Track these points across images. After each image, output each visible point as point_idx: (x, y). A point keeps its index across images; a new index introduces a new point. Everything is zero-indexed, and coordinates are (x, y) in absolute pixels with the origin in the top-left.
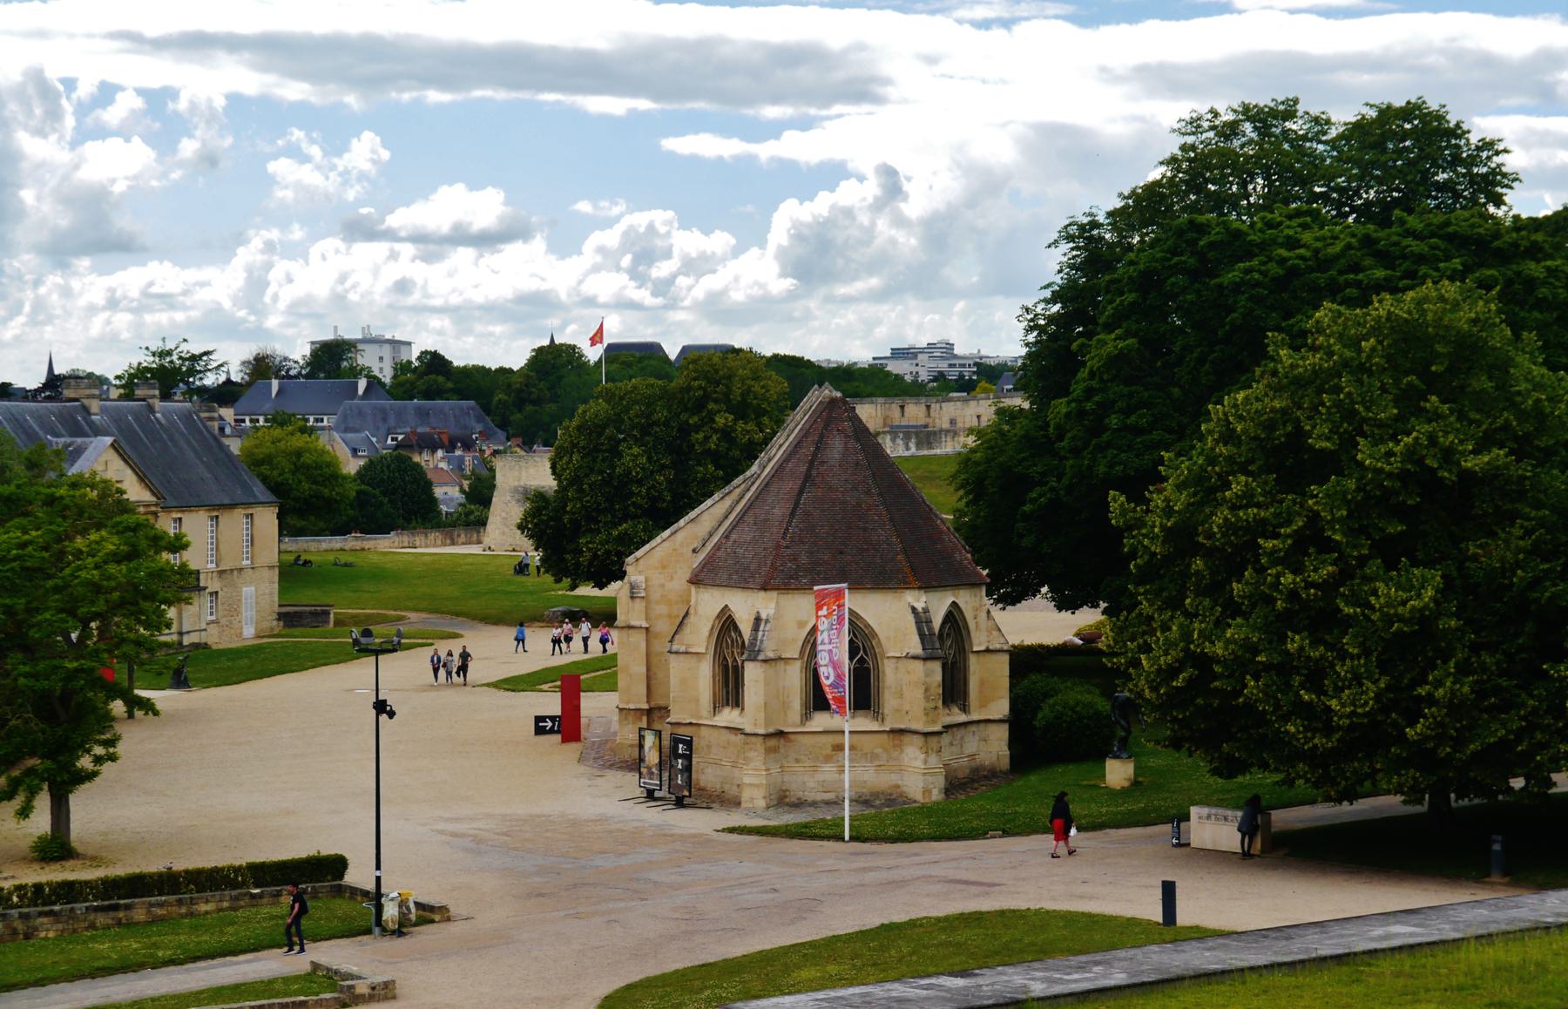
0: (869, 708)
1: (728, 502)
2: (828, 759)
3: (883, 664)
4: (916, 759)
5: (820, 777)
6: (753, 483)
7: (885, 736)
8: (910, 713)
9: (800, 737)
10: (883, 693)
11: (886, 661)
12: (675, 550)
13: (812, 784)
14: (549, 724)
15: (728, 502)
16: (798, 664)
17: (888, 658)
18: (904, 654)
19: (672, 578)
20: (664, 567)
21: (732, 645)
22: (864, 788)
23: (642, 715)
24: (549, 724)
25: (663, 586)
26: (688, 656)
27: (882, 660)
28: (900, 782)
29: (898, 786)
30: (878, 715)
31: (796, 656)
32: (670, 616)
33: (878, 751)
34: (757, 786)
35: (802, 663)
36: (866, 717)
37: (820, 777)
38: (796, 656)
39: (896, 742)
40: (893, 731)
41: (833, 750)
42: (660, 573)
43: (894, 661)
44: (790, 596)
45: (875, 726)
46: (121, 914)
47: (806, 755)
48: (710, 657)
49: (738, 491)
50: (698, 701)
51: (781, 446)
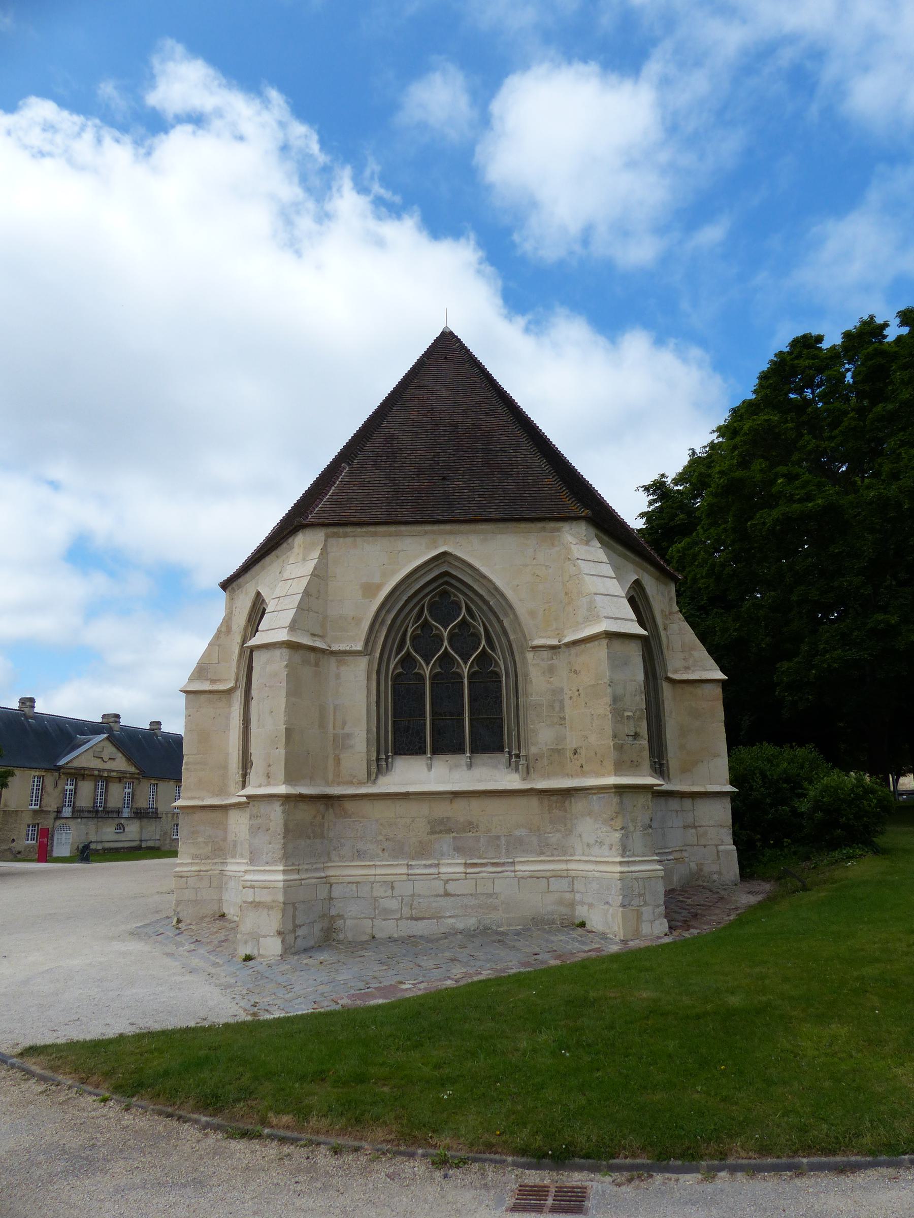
0: (500, 749)
3: (524, 659)
7: (534, 801)
8: (583, 752)
11: (530, 655)
17: (535, 648)
27: (522, 653)
31: (359, 647)
34: (268, 907)
35: (370, 663)
38: (359, 647)
43: (545, 654)
44: (349, 540)
45: (512, 781)
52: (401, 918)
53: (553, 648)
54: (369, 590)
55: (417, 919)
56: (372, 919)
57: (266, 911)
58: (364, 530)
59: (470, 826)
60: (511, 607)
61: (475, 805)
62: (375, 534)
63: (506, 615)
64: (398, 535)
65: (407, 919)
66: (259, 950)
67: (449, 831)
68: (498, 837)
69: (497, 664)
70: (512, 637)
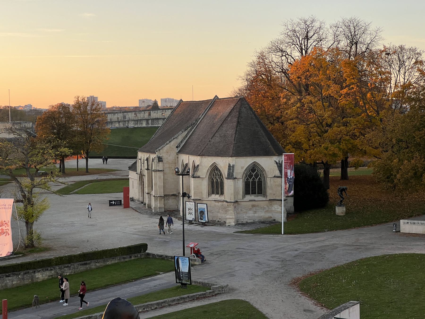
0: (262, 193)
1: (186, 132)
2: (250, 209)
4: (278, 209)
5: (248, 215)
6: (195, 126)
7: (267, 202)
9: (242, 203)
10: (267, 188)
11: (267, 179)
13: (246, 218)
14: (114, 203)
15: (186, 132)
16: (241, 180)
18: (273, 176)
19: (170, 156)
20: (167, 152)
23: (162, 198)
24: (114, 203)
25: (167, 158)
26: (199, 178)
28: (272, 216)
29: (271, 217)
30: (265, 195)
31: (241, 178)
32: (169, 168)
37: (248, 215)
40: (270, 200)
41: (252, 207)
42: (166, 154)
46: (88, 266)
48: (207, 179)
49: (189, 128)
50: (202, 193)
51: (203, 114)
54: (242, 168)
59: (258, 206)
63: (264, 172)
67: (254, 207)
68: (262, 208)
70: (265, 175)
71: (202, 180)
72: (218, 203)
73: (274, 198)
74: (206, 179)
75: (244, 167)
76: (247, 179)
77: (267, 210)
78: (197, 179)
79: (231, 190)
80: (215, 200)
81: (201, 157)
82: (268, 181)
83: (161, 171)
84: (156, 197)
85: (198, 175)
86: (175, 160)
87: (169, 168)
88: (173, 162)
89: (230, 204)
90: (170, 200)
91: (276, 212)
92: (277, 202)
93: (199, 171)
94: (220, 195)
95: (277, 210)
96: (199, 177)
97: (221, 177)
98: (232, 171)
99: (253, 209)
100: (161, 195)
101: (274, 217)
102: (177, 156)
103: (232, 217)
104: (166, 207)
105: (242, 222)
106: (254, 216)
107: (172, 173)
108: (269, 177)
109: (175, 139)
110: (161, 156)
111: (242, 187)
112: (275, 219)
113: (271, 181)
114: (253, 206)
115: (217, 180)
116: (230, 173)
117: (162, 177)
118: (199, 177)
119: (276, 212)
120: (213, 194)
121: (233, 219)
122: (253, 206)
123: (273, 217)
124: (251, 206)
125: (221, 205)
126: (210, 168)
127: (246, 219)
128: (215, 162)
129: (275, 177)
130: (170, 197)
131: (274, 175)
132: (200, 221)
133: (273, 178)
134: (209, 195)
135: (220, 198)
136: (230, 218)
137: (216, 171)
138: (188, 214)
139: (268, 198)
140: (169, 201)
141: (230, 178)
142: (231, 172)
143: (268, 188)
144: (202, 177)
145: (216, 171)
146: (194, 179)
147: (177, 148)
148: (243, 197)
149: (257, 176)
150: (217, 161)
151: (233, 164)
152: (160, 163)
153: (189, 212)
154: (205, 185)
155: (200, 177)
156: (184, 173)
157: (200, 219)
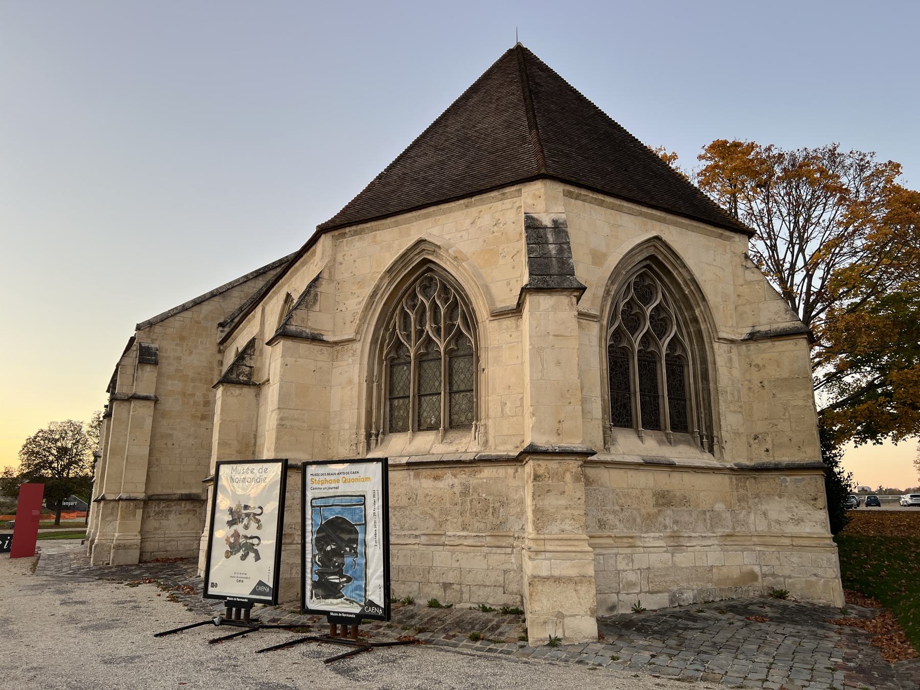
2: (649, 522)
4: (799, 521)
7: (723, 481)
11: (716, 345)
12: (197, 322)
13: (631, 577)
17: (719, 339)
20: (182, 339)
21: (421, 321)
22: (710, 581)
23: (136, 507)
25: (179, 358)
26: (315, 348)
28: (756, 569)
29: (753, 576)
30: (709, 442)
32: (183, 394)
33: (719, 507)
36: (689, 444)
37: (642, 559)
39: (742, 491)
40: (740, 470)
41: (657, 504)
43: (725, 347)
47: (614, 512)
48: (363, 348)
50: (326, 427)
52: (641, 592)
53: (732, 341)
54: (598, 258)
55: (652, 593)
56: (618, 593)
57: (572, 586)
58: (595, 196)
59: (685, 501)
60: (704, 299)
61: (689, 479)
62: (601, 204)
64: (619, 209)
65: (646, 592)
66: (564, 631)
67: (669, 504)
68: (704, 512)
69: (684, 350)
71: (334, 359)
72: (436, 478)
73: (765, 459)
74: (358, 346)
75: (605, 256)
76: (617, 335)
77: (728, 531)
78: (303, 348)
79: (558, 363)
80: (414, 459)
81: (336, 233)
82: (718, 359)
83: (146, 398)
84: (111, 505)
85: (310, 324)
86: (212, 369)
87: (183, 394)
88: (199, 374)
89: (553, 465)
90: (172, 517)
91: (787, 541)
92: (789, 480)
93: (317, 308)
94: (445, 430)
95: (791, 529)
96: (315, 339)
97: (459, 321)
98: (561, 251)
99: (660, 519)
100: (133, 495)
101: (773, 575)
102: (219, 357)
103: (573, 572)
104: (150, 546)
105: (612, 608)
106: (674, 566)
107: (194, 416)
108: (722, 335)
109: (216, 299)
110: (153, 346)
111: (601, 370)
112: (777, 588)
113: (730, 359)
114: (664, 499)
115: (429, 341)
116: (546, 256)
117: (149, 422)
118: (315, 339)
119: (787, 541)
120: (393, 429)
121: (583, 589)
122: (664, 499)
123: (764, 575)
124: (652, 501)
125: (458, 489)
126: (386, 281)
127: (631, 585)
128: (421, 241)
129: (754, 337)
130: (172, 504)
131: (749, 330)
132: (313, 604)
133: (744, 347)
134: (368, 436)
135: (452, 448)
136: (558, 580)
137: (420, 297)
138: (228, 555)
139: (727, 456)
140: (164, 523)
141: (552, 285)
142: (554, 252)
143: (721, 402)
144: (336, 339)
145: (420, 297)
146: (289, 343)
147: (221, 329)
148: (604, 433)
149: (660, 323)
150: (435, 231)
151: (554, 216)
152: (148, 368)
153: (236, 535)
154: (350, 382)
155: (325, 338)
156: (234, 376)
157: (315, 585)
